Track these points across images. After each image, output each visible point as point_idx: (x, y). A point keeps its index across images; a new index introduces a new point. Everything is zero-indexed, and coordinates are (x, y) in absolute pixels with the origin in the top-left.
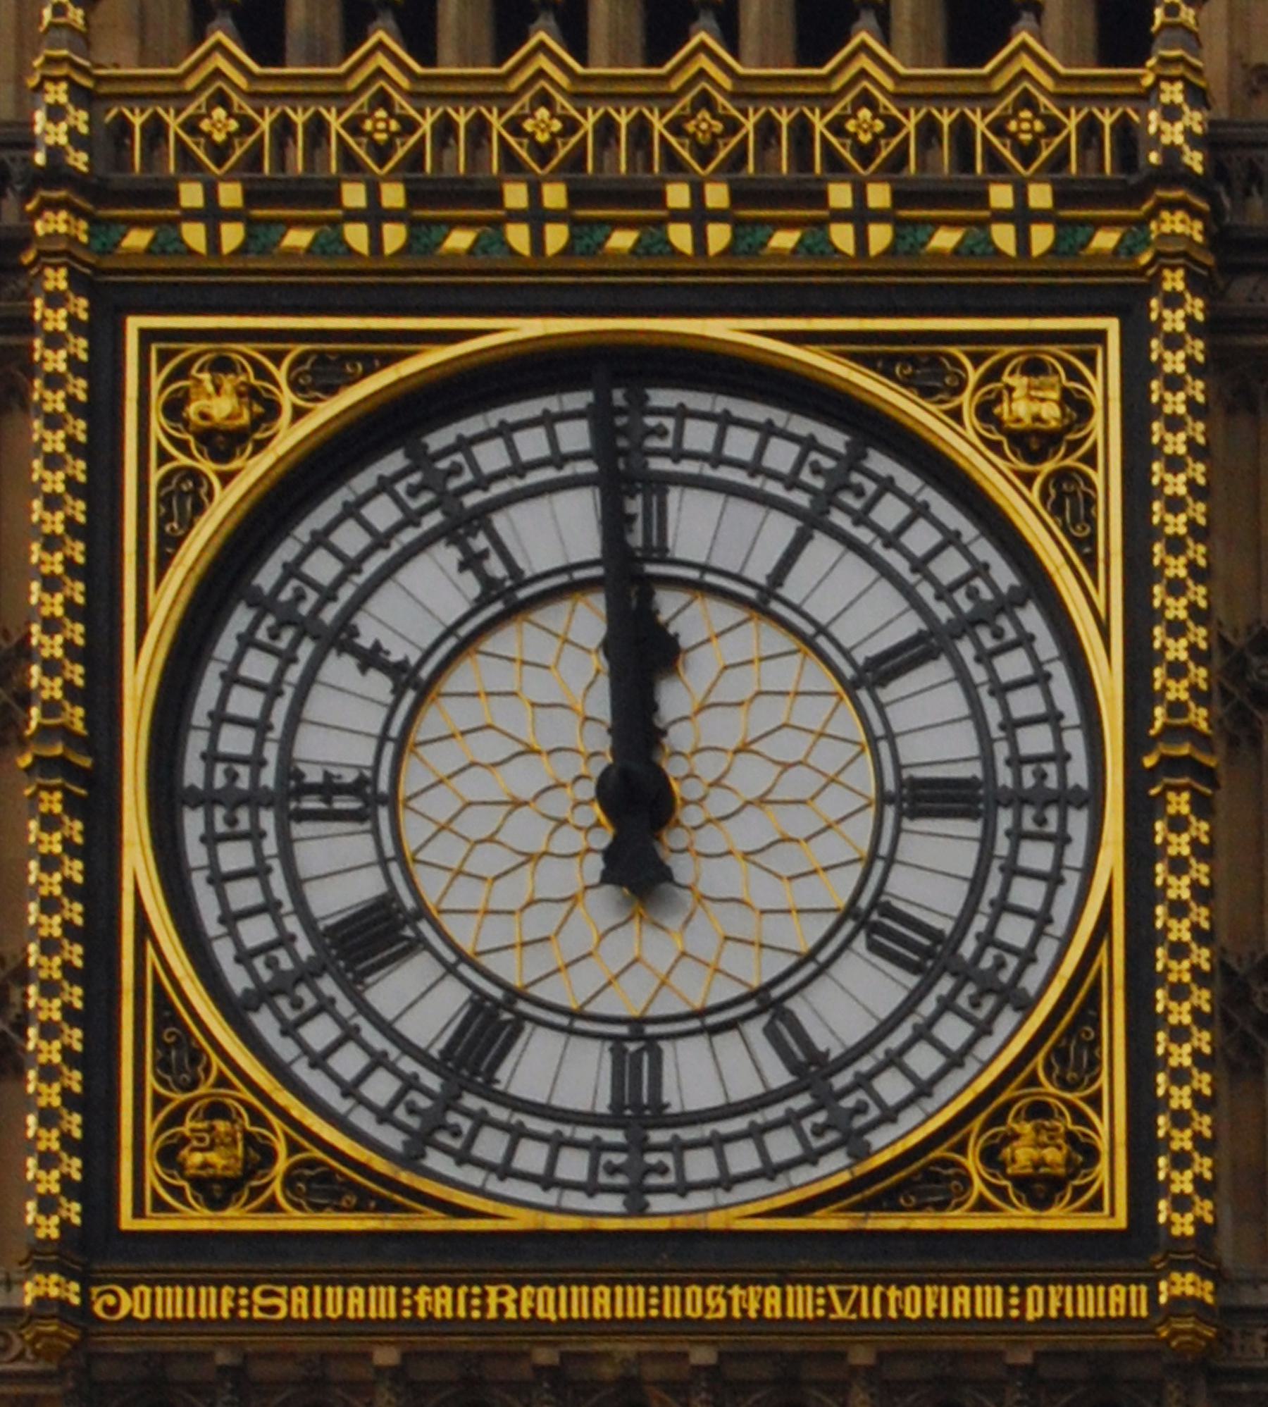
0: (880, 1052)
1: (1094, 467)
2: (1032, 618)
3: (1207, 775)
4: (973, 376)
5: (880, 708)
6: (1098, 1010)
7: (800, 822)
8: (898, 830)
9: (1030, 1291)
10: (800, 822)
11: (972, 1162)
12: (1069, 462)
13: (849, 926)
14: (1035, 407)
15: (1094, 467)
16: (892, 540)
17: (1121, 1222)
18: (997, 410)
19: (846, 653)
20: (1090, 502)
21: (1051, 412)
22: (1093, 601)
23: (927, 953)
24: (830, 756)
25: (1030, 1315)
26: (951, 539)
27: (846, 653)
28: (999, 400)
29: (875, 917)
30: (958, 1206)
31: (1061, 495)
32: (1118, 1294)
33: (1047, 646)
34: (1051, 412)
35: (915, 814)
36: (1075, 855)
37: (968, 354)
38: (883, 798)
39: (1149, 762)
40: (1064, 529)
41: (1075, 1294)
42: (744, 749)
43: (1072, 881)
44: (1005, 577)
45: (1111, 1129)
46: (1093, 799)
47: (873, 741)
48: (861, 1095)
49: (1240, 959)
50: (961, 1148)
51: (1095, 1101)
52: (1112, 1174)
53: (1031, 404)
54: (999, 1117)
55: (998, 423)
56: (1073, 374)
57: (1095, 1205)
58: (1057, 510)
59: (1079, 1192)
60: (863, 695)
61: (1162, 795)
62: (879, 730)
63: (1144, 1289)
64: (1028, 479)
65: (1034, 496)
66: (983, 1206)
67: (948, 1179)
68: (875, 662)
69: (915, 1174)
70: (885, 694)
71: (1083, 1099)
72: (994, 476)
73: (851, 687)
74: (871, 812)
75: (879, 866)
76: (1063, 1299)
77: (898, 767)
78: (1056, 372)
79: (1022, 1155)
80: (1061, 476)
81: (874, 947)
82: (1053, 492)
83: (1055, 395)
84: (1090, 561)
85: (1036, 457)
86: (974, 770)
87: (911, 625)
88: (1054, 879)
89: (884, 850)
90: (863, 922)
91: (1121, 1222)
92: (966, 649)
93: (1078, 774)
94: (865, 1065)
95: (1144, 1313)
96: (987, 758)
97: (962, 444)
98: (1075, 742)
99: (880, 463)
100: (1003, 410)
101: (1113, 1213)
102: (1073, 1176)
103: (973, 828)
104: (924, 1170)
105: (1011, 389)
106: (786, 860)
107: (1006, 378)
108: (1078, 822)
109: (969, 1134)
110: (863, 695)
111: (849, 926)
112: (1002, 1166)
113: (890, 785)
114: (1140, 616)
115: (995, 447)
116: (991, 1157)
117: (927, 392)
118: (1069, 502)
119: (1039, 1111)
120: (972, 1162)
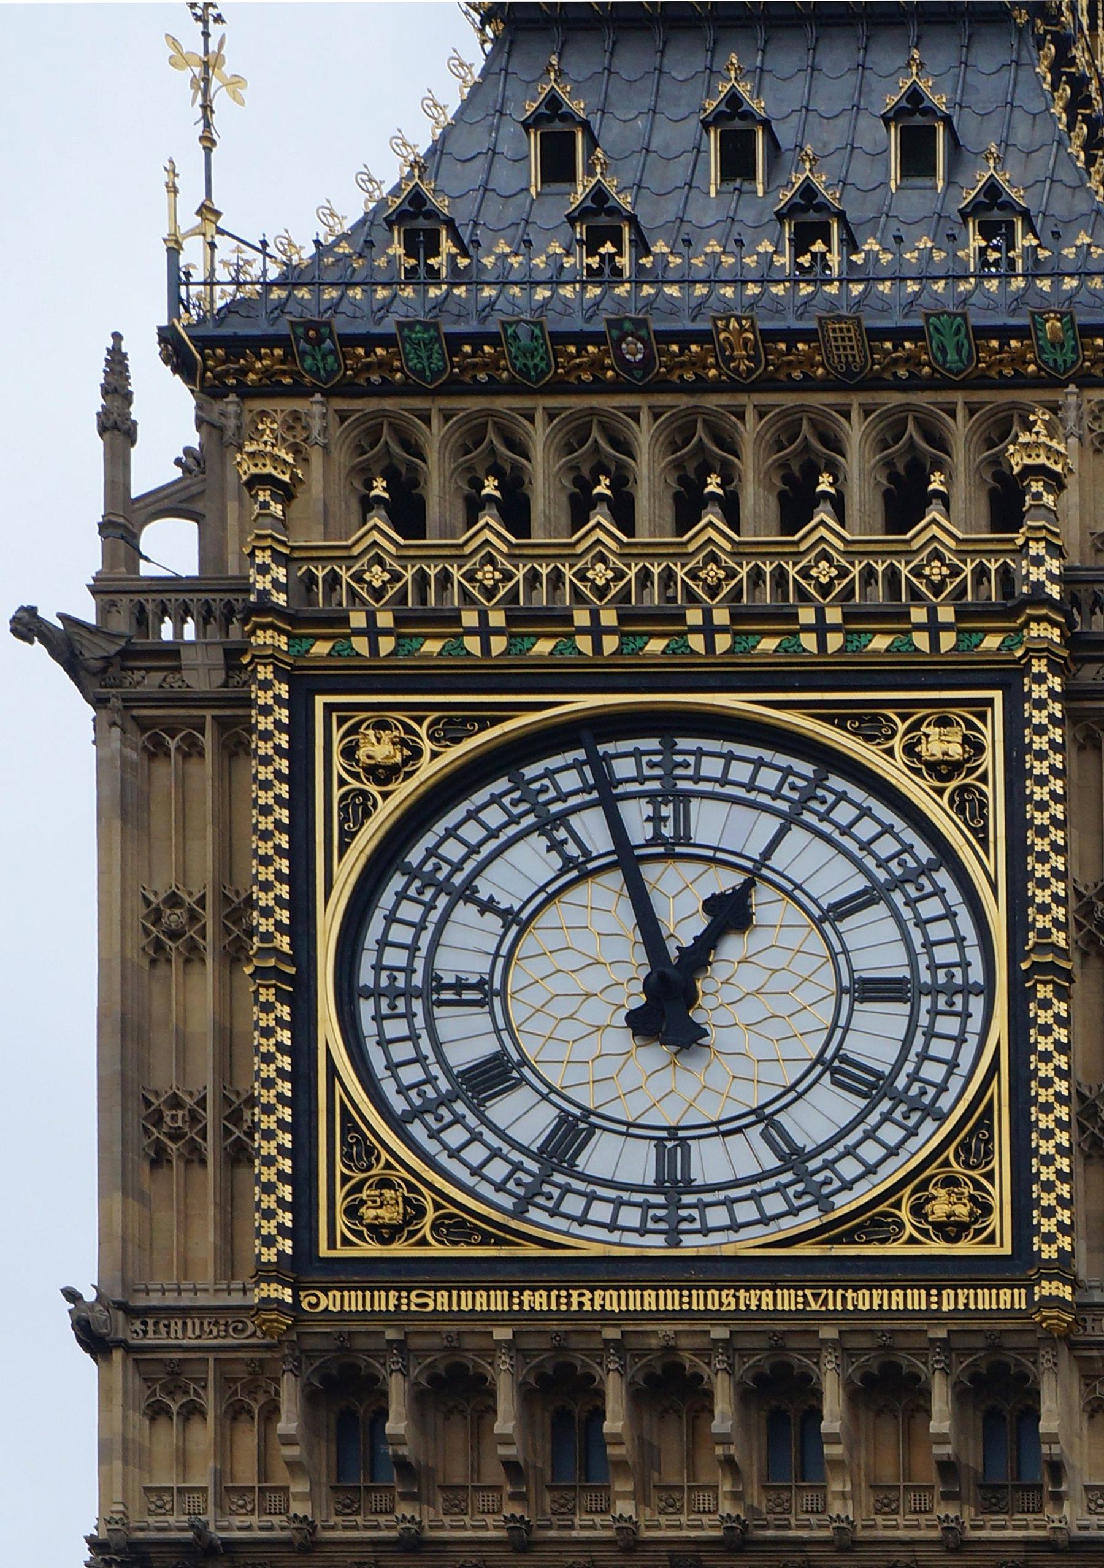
0: (840, 1147)
1: (986, 784)
2: (943, 878)
3: (1068, 975)
4: (902, 728)
5: (839, 935)
6: (991, 1119)
7: (782, 1006)
8: (852, 1010)
9: (944, 1293)
10: (782, 1006)
11: (904, 1214)
12: (968, 780)
13: (819, 1069)
14: (945, 746)
15: (986, 784)
16: (845, 831)
17: (1007, 1250)
18: (917, 749)
19: (815, 901)
20: (983, 805)
21: (956, 751)
22: (988, 867)
23: (873, 1086)
24: (804, 965)
25: (945, 1308)
26: (887, 829)
27: (815, 901)
28: (919, 742)
29: (836, 1063)
30: (895, 1241)
31: (963, 802)
32: (1005, 1295)
33: (954, 895)
34: (956, 751)
35: (863, 1000)
36: (975, 1024)
37: (898, 714)
38: (841, 990)
39: (1024, 966)
40: (965, 822)
41: (976, 1295)
42: (745, 961)
43: (973, 1041)
44: (925, 853)
45: (1000, 1193)
46: (988, 990)
47: (834, 955)
48: (828, 1173)
49: (1091, 1090)
50: (897, 1205)
51: (990, 1176)
52: (1001, 1221)
53: (941, 744)
54: (924, 1186)
55: (919, 756)
56: (970, 725)
57: (990, 1240)
58: (960, 811)
59: (979, 1232)
60: (827, 926)
61: (1034, 986)
62: (838, 948)
63: (1023, 1291)
64: (940, 792)
65: (944, 802)
66: (912, 1240)
67: (888, 1225)
68: (834, 907)
69: (865, 1221)
70: (841, 926)
71: (982, 1175)
72: (917, 791)
73: (818, 922)
74: (833, 998)
75: (839, 1032)
76: (967, 1298)
77: (851, 971)
78: (958, 724)
79: (939, 1210)
80: (963, 789)
81: (835, 1082)
82: (957, 799)
83: (959, 739)
84: (984, 842)
85: (948, 778)
86: (905, 973)
87: (860, 883)
88: (960, 1040)
89: (842, 1022)
90: (828, 1067)
91: (1007, 1250)
92: (898, 897)
93: (977, 974)
94: (830, 1154)
95: (1024, 1306)
96: (913, 965)
97: (894, 771)
98: (974, 955)
99: (836, 782)
100: (921, 748)
101: (1002, 1245)
102: (975, 1223)
103: (905, 1008)
104: (871, 1218)
105: (927, 736)
106: (774, 1029)
107: (923, 729)
108: (977, 1005)
109: (901, 1198)
110: (827, 926)
111: (819, 1069)
112: (926, 1216)
113: (846, 982)
114: (1018, 876)
115: (917, 772)
116: (917, 1210)
117: (869, 739)
118: (972, 806)
119: (951, 1182)
120: (904, 1214)
